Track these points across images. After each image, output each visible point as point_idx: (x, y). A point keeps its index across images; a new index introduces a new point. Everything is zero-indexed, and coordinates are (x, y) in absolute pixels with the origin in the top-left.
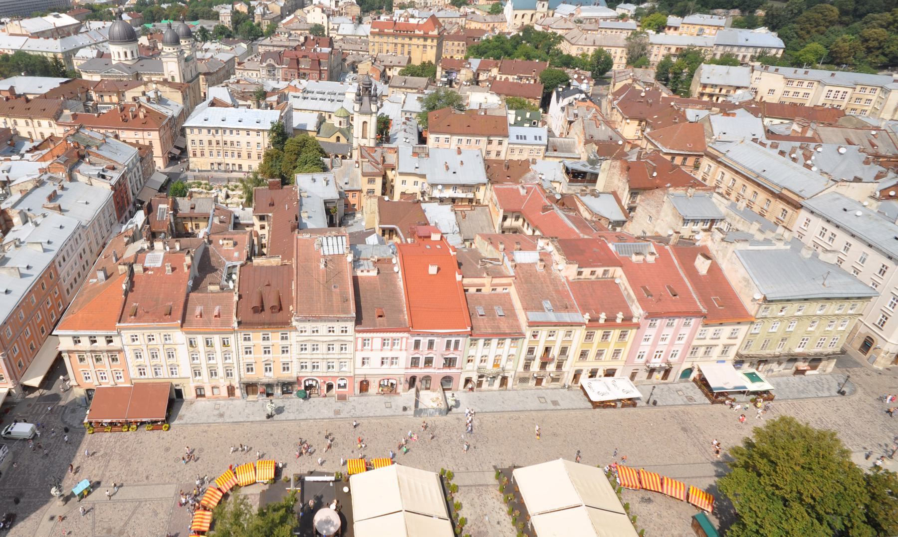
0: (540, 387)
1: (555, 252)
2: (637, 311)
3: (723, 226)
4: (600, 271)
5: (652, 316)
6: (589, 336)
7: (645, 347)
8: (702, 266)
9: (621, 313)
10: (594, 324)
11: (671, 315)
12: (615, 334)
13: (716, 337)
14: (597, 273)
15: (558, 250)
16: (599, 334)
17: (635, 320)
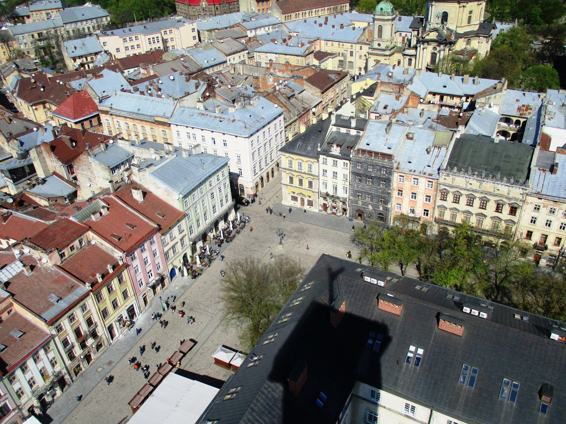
0: (93, 361)
1: (33, 251)
2: (118, 254)
3: (135, 161)
4: (76, 243)
5: (129, 253)
6: (99, 298)
7: (140, 276)
8: (137, 195)
9: (109, 266)
10: (96, 286)
11: (139, 244)
12: (115, 283)
13: (172, 239)
14: (75, 246)
15: (34, 248)
16: (104, 291)
17: (121, 263)
